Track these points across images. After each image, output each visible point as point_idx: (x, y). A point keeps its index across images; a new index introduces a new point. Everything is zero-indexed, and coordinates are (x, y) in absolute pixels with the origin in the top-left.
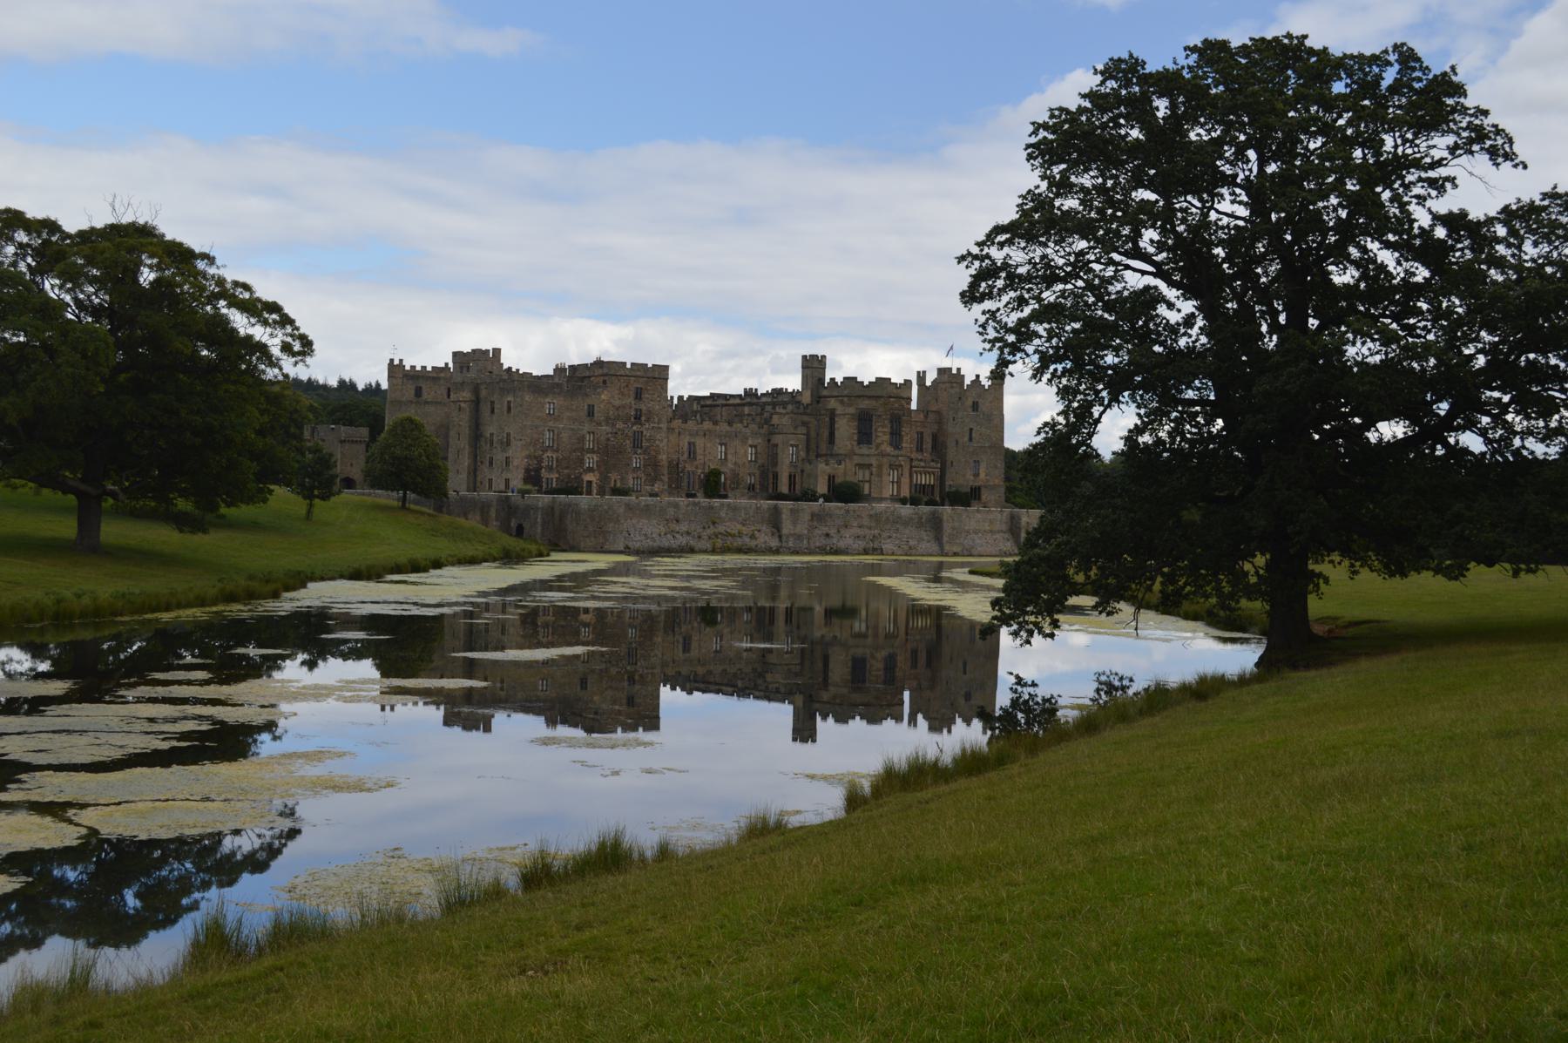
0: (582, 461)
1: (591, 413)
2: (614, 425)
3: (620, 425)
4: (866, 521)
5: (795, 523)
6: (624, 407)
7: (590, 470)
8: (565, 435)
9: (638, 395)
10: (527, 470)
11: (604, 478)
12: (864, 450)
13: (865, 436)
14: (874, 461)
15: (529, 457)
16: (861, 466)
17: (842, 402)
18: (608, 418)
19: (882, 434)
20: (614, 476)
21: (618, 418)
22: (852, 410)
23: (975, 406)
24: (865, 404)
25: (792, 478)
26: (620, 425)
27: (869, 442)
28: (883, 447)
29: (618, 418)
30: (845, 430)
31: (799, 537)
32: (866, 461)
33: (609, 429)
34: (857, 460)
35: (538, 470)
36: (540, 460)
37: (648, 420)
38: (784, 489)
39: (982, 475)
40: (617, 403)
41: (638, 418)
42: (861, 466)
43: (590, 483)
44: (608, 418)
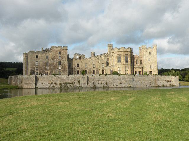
0: (45, 68)
1: (47, 57)
3: (55, 60)
5: (84, 80)
6: (56, 56)
7: (48, 70)
8: (41, 63)
9: (60, 53)
10: (31, 71)
11: (51, 72)
12: (119, 64)
13: (119, 60)
14: (121, 66)
16: (118, 67)
17: (114, 54)
19: (123, 60)
20: (54, 71)
22: (116, 55)
23: (150, 53)
24: (119, 53)
25: (103, 71)
26: (55, 60)
30: (116, 59)
32: (119, 66)
33: (52, 61)
36: (34, 68)
38: (101, 72)
40: (54, 55)
42: (118, 67)
43: (47, 73)
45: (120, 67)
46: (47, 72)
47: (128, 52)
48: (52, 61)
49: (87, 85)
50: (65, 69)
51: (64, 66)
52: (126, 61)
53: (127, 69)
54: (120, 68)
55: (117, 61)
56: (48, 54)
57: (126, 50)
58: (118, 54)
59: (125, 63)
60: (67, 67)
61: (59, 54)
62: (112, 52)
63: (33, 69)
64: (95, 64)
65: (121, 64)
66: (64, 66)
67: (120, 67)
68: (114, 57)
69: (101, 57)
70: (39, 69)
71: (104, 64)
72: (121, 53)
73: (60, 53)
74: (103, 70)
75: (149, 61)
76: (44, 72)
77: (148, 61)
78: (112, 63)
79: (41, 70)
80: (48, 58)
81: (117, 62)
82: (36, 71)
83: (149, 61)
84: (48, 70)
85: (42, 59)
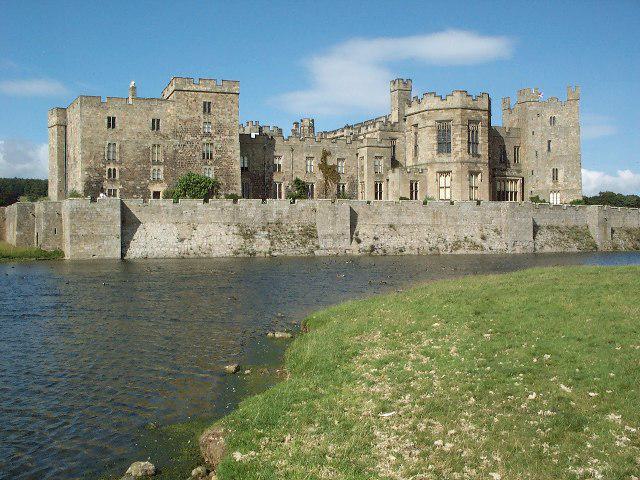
0: (147, 173)
1: (156, 124)
3: (188, 137)
6: (192, 120)
7: (158, 180)
9: (207, 108)
12: (444, 158)
13: (444, 145)
14: (453, 168)
17: (423, 117)
19: (458, 142)
22: (430, 123)
24: (444, 115)
26: (188, 137)
27: (449, 151)
28: (460, 155)
30: (428, 139)
33: (177, 142)
34: (437, 168)
40: (185, 117)
44: (175, 133)
45: (449, 172)
46: (154, 188)
51: (224, 163)
52: (472, 143)
53: (477, 180)
55: (436, 148)
56: (156, 113)
57: (471, 103)
58: (440, 119)
59: (467, 157)
60: (237, 168)
61: (205, 111)
64: (343, 160)
65: (452, 159)
66: (224, 163)
69: (363, 130)
71: (381, 158)
72: (456, 116)
73: (207, 108)
80: (158, 128)
84: (158, 180)
85: (132, 132)
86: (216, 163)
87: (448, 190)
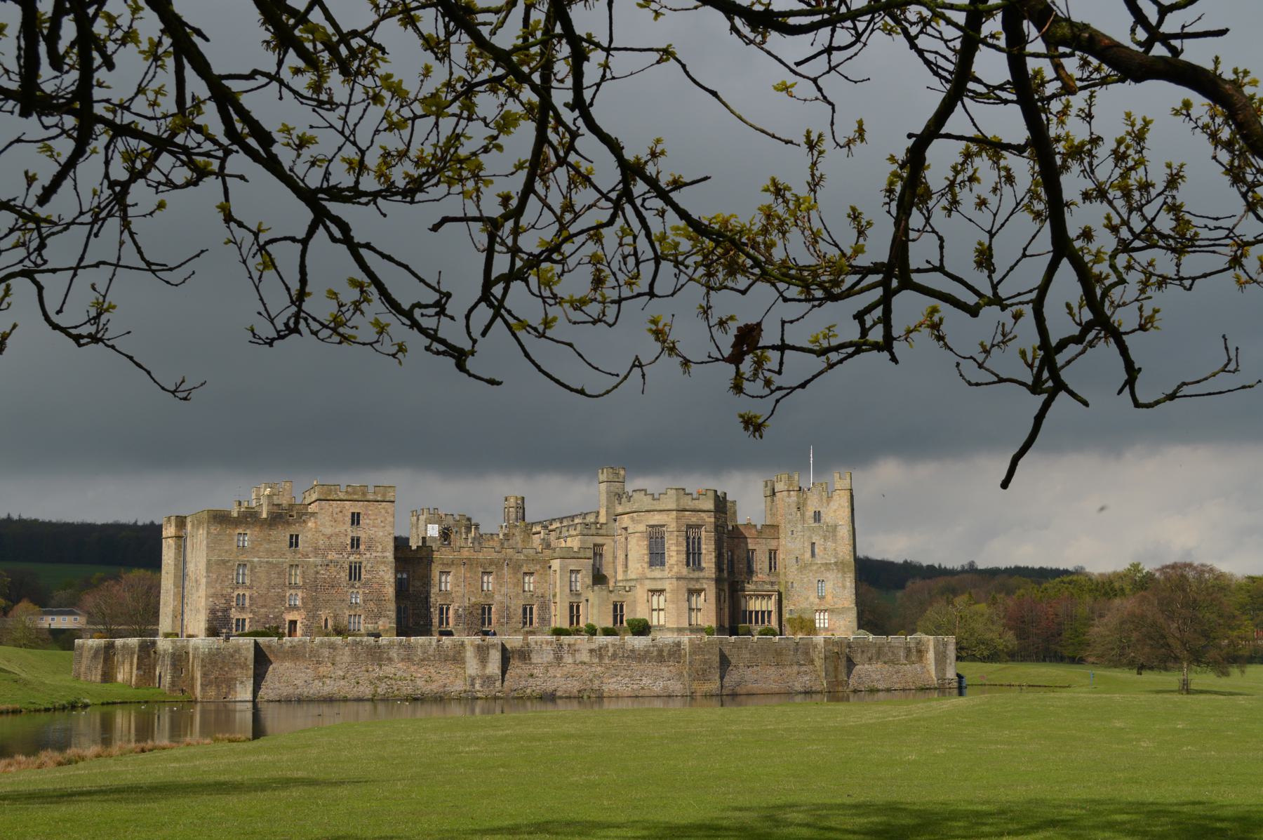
2: (324, 556)
4: (585, 657)
6: (337, 535)
7: (295, 608)
10: (213, 611)
11: (312, 615)
12: (657, 573)
13: (656, 557)
14: (667, 585)
15: (214, 595)
16: (653, 591)
17: (633, 519)
18: (316, 549)
19: (674, 552)
21: (330, 548)
23: (817, 516)
24: (656, 519)
25: (574, 612)
26: (332, 556)
27: (663, 564)
29: (330, 548)
30: (638, 549)
31: (488, 680)
32: (659, 586)
35: (226, 610)
37: (369, 548)
39: (829, 598)
40: (329, 531)
41: (356, 543)
45: (661, 591)
46: (289, 617)
47: (703, 514)
48: (319, 560)
49: (498, 684)
50: (379, 600)
51: (375, 586)
52: (692, 556)
53: (699, 601)
54: (662, 598)
55: (647, 559)
60: (390, 591)
61: (353, 523)
62: (620, 509)
63: (221, 603)
64: (532, 574)
65: (666, 574)
66: (375, 586)
67: (661, 591)
68: (633, 541)
69: (565, 533)
70: (251, 605)
71: (578, 571)
72: (669, 520)
74: (571, 607)
75: (813, 554)
76: (275, 618)
77: (808, 555)
78: (620, 569)
79: (263, 607)
80: (297, 545)
81: (646, 565)
82: (234, 614)
83: (813, 554)
84: (295, 608)
86: (365, 585)
87: (662, 613)
